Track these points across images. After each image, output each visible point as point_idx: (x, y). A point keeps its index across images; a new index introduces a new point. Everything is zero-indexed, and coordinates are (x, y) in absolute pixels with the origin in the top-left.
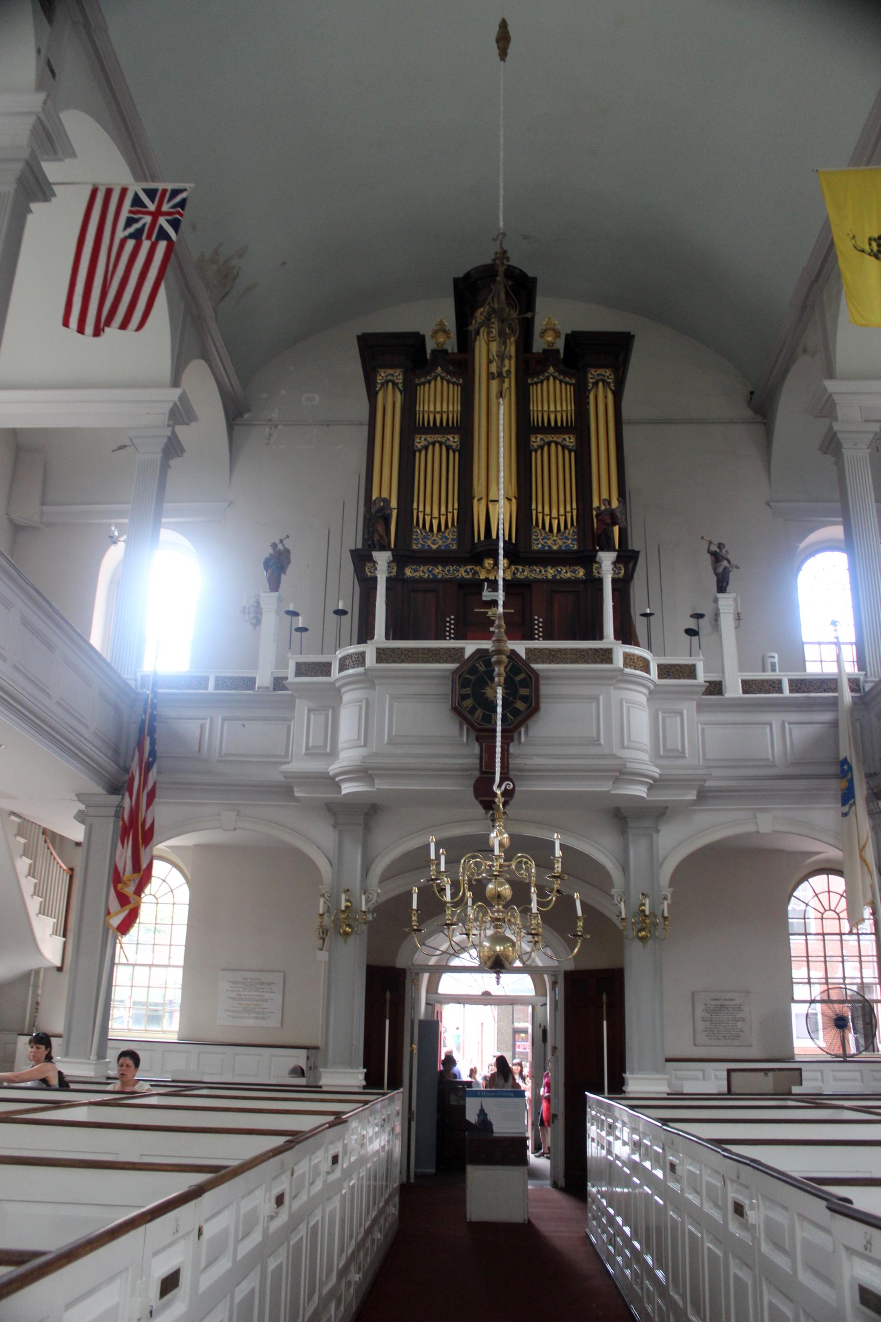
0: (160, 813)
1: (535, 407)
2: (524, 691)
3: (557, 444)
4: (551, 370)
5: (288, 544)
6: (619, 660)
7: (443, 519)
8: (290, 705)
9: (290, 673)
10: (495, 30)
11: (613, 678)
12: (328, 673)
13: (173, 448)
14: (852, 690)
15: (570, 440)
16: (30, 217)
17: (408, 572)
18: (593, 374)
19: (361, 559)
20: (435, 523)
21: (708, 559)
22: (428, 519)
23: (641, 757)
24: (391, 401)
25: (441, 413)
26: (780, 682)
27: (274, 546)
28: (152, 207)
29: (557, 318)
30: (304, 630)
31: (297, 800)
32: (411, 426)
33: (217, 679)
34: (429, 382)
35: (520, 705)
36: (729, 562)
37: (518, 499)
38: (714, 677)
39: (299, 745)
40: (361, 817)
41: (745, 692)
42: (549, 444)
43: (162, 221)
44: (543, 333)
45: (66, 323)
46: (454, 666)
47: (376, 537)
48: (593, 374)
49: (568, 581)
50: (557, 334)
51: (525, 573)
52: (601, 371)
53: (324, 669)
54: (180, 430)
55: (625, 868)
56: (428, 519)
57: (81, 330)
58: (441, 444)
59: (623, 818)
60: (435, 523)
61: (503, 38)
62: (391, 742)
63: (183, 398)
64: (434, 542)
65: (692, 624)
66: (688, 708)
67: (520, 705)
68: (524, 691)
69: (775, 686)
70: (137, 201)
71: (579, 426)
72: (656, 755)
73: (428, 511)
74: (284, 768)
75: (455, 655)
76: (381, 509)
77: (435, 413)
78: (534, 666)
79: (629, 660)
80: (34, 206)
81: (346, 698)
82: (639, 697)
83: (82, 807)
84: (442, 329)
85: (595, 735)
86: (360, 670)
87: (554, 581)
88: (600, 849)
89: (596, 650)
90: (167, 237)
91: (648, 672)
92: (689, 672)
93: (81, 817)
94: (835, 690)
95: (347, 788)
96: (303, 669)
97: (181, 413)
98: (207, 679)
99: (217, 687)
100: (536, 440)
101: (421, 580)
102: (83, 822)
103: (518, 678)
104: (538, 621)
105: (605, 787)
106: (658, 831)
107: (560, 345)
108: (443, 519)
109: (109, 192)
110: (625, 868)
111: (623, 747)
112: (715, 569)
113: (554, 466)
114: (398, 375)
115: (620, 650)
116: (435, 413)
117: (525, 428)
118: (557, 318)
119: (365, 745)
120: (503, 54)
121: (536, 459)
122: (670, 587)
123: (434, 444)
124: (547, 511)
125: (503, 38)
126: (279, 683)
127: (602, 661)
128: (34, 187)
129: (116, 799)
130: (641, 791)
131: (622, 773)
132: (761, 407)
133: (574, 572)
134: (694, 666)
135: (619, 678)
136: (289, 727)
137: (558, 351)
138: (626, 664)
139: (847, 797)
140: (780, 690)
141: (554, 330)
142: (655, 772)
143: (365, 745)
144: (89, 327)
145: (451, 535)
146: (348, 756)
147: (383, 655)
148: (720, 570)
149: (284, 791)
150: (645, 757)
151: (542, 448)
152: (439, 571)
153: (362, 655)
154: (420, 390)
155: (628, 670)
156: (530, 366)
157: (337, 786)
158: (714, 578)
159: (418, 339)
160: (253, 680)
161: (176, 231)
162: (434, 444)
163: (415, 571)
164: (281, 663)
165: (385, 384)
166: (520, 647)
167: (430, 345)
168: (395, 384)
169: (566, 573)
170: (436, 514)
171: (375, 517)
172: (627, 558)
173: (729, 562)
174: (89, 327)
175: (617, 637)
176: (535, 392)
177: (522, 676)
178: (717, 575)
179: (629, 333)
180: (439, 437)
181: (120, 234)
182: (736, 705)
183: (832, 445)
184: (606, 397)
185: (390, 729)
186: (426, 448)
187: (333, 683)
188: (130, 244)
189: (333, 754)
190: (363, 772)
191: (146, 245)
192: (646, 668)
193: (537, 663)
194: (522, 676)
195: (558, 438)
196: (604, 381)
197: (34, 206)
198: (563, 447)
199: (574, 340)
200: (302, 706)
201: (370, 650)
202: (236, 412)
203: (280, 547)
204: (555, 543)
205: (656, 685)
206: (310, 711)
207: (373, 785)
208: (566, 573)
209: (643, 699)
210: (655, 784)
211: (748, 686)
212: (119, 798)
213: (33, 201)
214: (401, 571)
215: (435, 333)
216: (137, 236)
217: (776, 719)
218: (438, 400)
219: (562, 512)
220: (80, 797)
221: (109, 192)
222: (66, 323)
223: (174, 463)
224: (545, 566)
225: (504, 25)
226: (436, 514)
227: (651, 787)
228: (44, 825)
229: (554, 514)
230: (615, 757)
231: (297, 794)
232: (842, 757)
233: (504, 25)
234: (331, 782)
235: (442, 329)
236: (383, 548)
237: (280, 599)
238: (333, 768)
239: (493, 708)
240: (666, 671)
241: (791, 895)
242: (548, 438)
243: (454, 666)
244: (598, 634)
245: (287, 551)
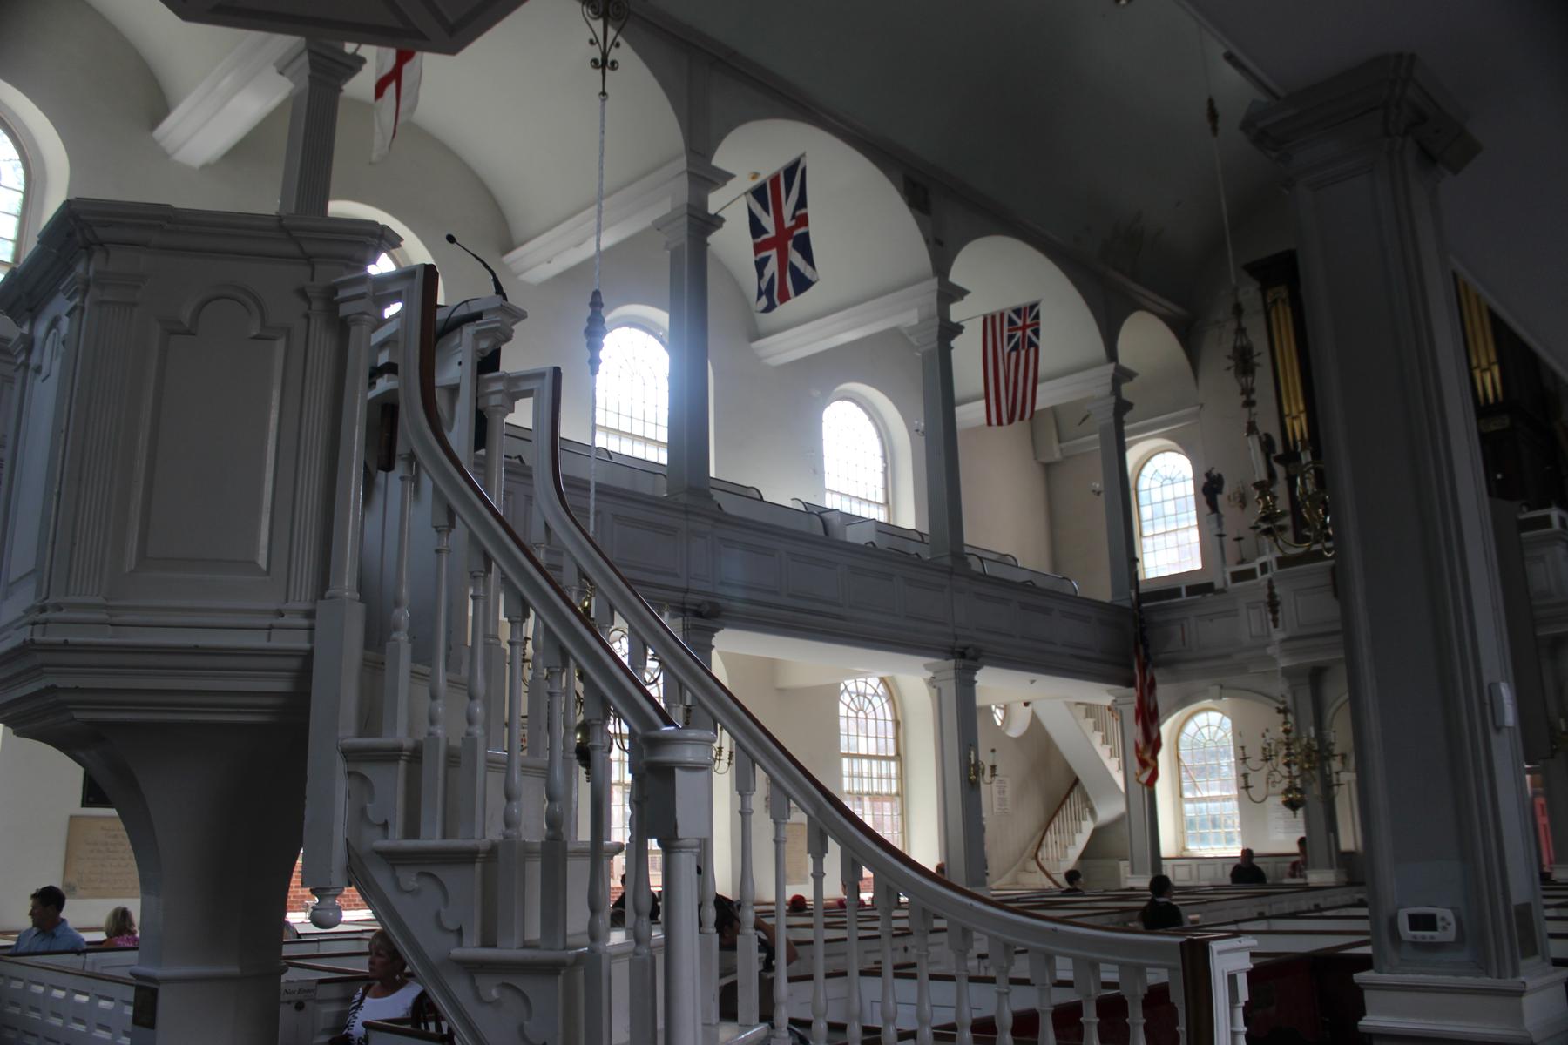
10: (1205, 107)
13: (1122, 408)
16: (953, 352)
43: (1029, 332)
57: (1000, 423)
61: (1213, 115)
70: (1011, 322)
95: (1284, 663)
96: (1237, 577)
97: (1122, 376)
109: (993, 317)
120: (1215, 130)
125: (1213, 115)
128: (949, 331)
144: (1005, 420)
165: (1275, 302)
174: (1005, 420)
181: (1007, 350)
188: (1014, 354)
191: (1023, 353)
216: (1016, 348)
225: (1211, 102)
233: (1211, 102)
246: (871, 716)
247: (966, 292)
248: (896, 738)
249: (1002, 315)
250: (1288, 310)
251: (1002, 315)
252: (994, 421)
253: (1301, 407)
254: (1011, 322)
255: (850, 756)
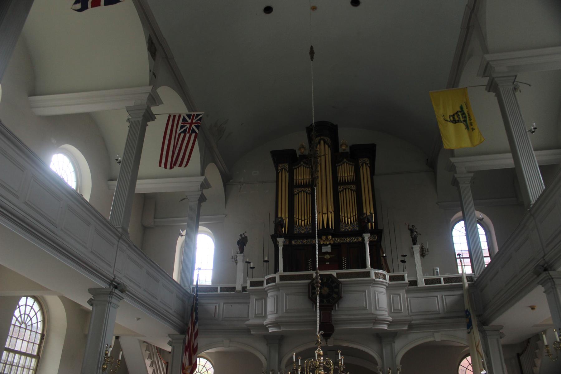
0: (201, 341)
1: (339, 175)
2: (336, 290)
3: (348, 189)
4: (345, 160)
5: (246, 234)
6: (373, 276)
7: (306, 221)
8: (248, 297)
9: (248, 285)
11: (370, 283)
12: (262, 285)
13: (202, 199)
14: (468, 281)
15: (353, 187)
17: (293, 242)
18: (361, 161)
19: (274, 238)
20: (303, 223)
21: (409, 232)
22: (300, 221)
23: (384, 313)
24: (284, 177)
25: (304, 179)
26: (440, 279)
27: (241, 235)
28: (189, 121)
29: (347, 138)
30: (253, 268)
31: (252, 335)
32: (292, 185)
33: (221, 288)
34: (298, 168)
35: (335, 296)
36: (417, 232)
37: (334, 212)
38: (412, 279)
39: (252, 313)
40: (276, 341)
41: (426, 284)
42: (346, 189)
43: (193, 126)
44: (342, 145)
45: (160, 165)
46: (310, 281)
47: (278, 233)
48: (361, 161)
49: (355, 243)
50: (346, 145)
51: (338, 240)
52: (364, 159)
53: (261, 283)
54: (205, 191)
55: (382, 357)
56: (300, 221)
57: (165, 167)
58: (304, 191)
59: (381, 338)
60: (303, 223)
61: (312, 53)
62: (287, 312)
63: (205, 180)
64: (303, 230)
65: (402, 258)
66: (402, 293)
67: (335, 296)
68: (336, 290)
69: (438, 281)
70: (184, 119)
71: (357, 181)
72: (390, 312)
73: (300, 218)
74: (247, 322)
75: (310, 277)
76: (280, 222)
77: (301, 179)
78: (339, 280)
79: (377, 275)
80: (148, 123)
81: (269, 294)
82: (383, 289)
83: (171, 339)
84: (302, 147)
85: (365, 306)
86: (274, 284)
87: (350, 243)
88: (371, 350)
89: (364, 272)
90: (195, 132)
91: (385, 279)
92: (402, 278)
93: (170, 343)
94: (461, 281)
95: (271, 330)
96: (253, 284)
97: (205, 185)
98: (217, 288)
99: (221, 291)
100: (340, 188)
101: (298, 245)
102: (171, 345)
103: (333, 285)
104: (344, 259)
105: (370, 326)
106: (394, 342)
107: (348, 150)
108: (306, 221)
109: (174, 116)
110: (382, 357)
111: (376, 310)
112: (411, 235)
113: (348, 198)
114: (286, 166)
115: (373, 272)
116: (301, 179)
117: (336, 183)
118: (347, 138)
119: (277, 313)
120: (312, 58)
121: (341, 195)
122: (396, 243)
123: (301, 192)
124: (346, 215)
125: (312, 53)
126: (244, 289)
127: (366, 277)
128: (149, 117)
129: (183, 336)
130: (385, 327)
131: (376, 320)
132: (431, 165)
133: (357, 239)
134: (404, 276)
135: (374, 283)
136: (249, 306)
137: (347, 152)
138: (376, 277)
139: (469, 325)
140: (440, 283)
141: (345, 144)
142: (390, 319)
143: (277, 313)
144: (168, 167)
145: (309, 227)
146: (271, 318)
147: (282, 278)
148: (413, 236)
149: (247, 331)
150: (386, 313)
151: (343, 191)
152: (305, 241)
153: (275, 278)
154: (295, 171)
155: (377, 279)
156: (337, 158)
157: (267, 329)
158: (411, 239)
159: (293, 152)
160: (235, 288)
161: (198, 130)
162: (301, 192)
163: (296, 242)
164: (245, 281)
165: (281, 170)
166: (334, 273)
167: (298, 153)
168: (285, 169)
169: (354, 240)
170: (303, 219)
171: (279, 224)
172: (377, 233)
173: (417, 232)
174: (168, 167)
175: (371, 267)
176: (339, 169)
177: (335, 284)
178: (412, 238)
179: (373, 144)
180: (303, 189)
181: (178, 132)
182: (423, 290)
183: (455, 183)
184: (367, 169)
185: (286, 307)
186: (298, 193)
187: (264, 289)
188: (182, 135)
189: (265, 317)
190: (276, 324)
191: (188, 135)
192: (385, 278)
193: (341, 278)
194: (335, 284)
195: (349, 186)
196: (366, 163)
197: (148, 123)
198: (351, 190)
199: (353, 147)
200: (253, 298)
201: (277, 276)
202: (227, 180)
203: (243, 236)
204: (349, 228)
205: (389, 284)
206: (256, 300)
207: (280, 329)
208: (354, 240)
209: (384, 290)
210: (391, 324)
211: (427, 282)
212: (184, 336)
213: (149, 121)
214: (290, 242)
215: (300, 149)
216: (184, 132)
217: (439, 294)
218: (302, 175)
219: (352, 215)
220: (170, 336)
221: (174, 116)
222: (160, 165)
223: (203, 204)
224: (346, 238)
226: (303, 219)
227: (389, 325)
228: (156, 346)
229: (349, 216)
230: (373, 314)
231: (252, 333)
232: (466, 309)
234: (265, 328)
235: (302, 147)
236: (281, 237)
237: (244, 256)
238: (265, 322)
239: (328, 296)
240: (392, 278)
241: (459, 364)
242: (345, 187)
243: (310, 281)
244: (365, 266)
245: (246, 237)
246: (29, 328)
247: (162, 103)
248: (40, 345)
249: (180, 116)
250: (287, 174)
251: (180, 116)
252: (163, 165)
253: (287, 216)
254: (184, 119)
255: (9, 350)
